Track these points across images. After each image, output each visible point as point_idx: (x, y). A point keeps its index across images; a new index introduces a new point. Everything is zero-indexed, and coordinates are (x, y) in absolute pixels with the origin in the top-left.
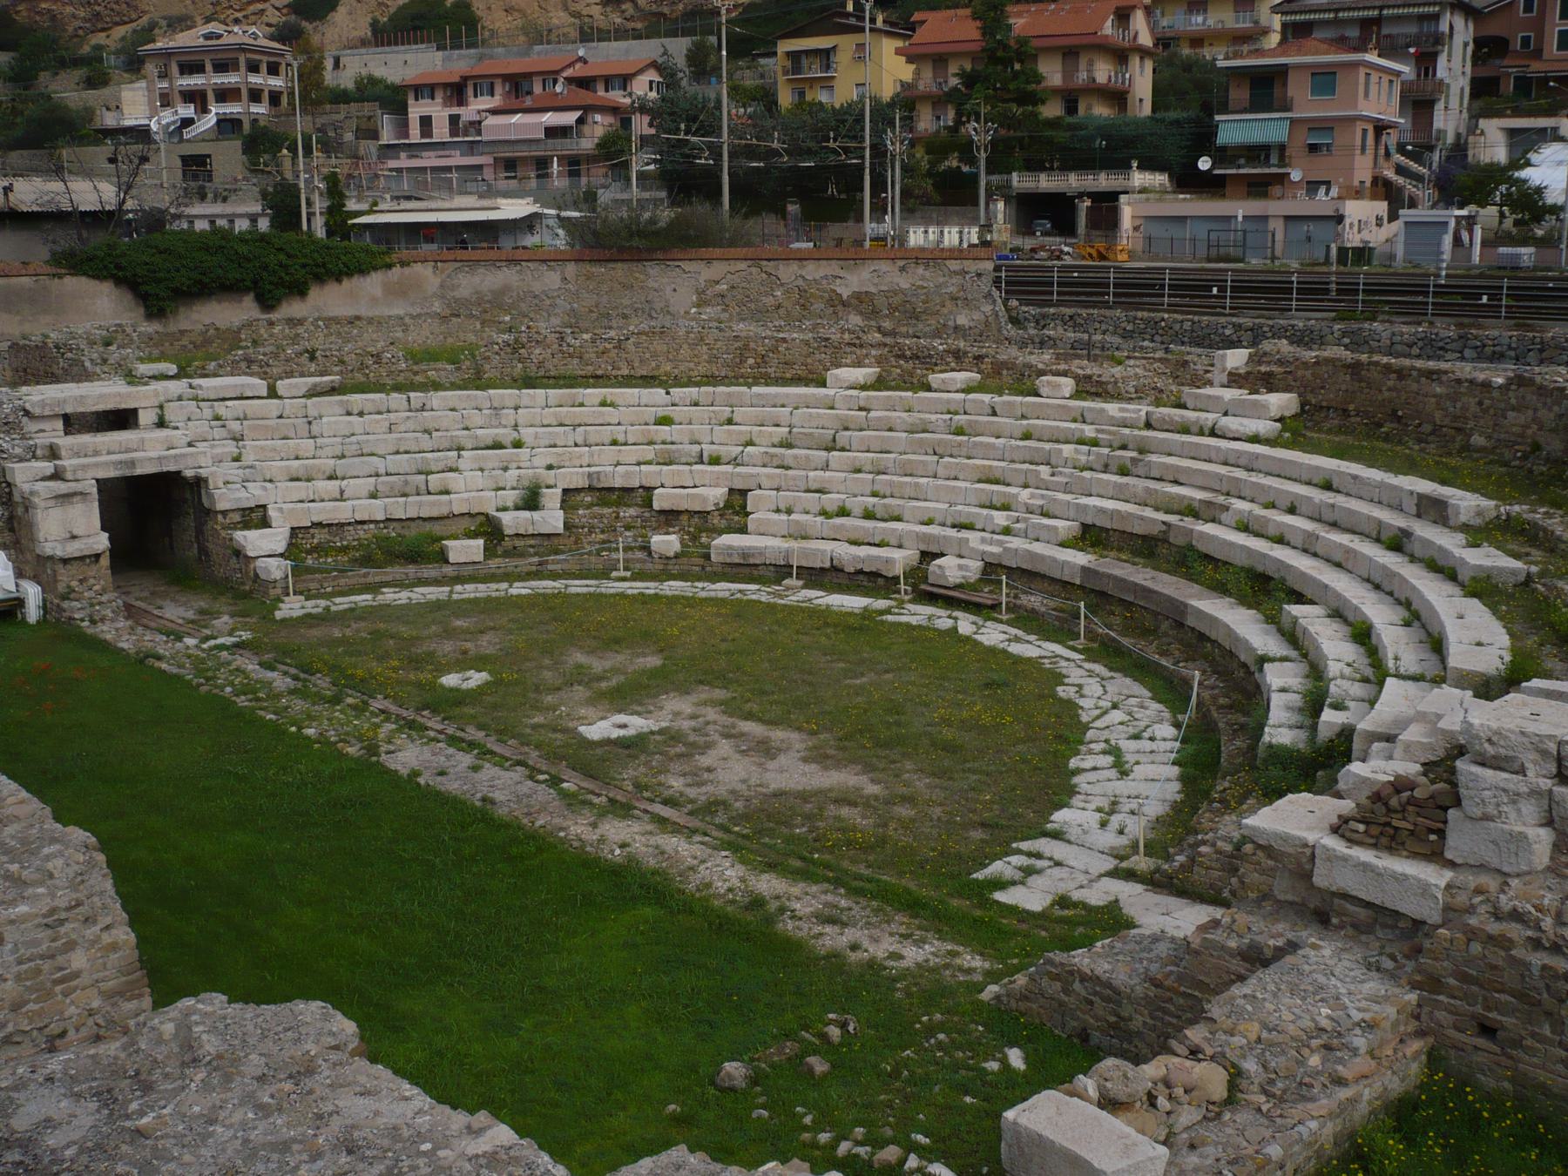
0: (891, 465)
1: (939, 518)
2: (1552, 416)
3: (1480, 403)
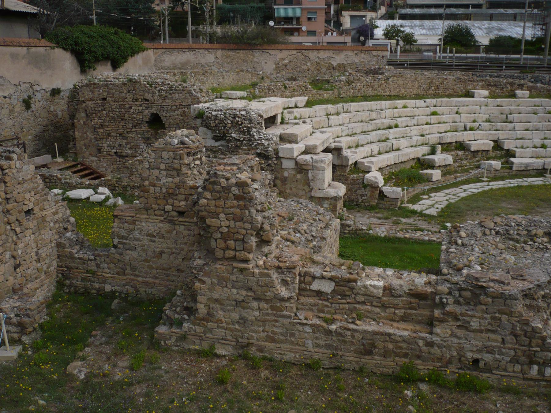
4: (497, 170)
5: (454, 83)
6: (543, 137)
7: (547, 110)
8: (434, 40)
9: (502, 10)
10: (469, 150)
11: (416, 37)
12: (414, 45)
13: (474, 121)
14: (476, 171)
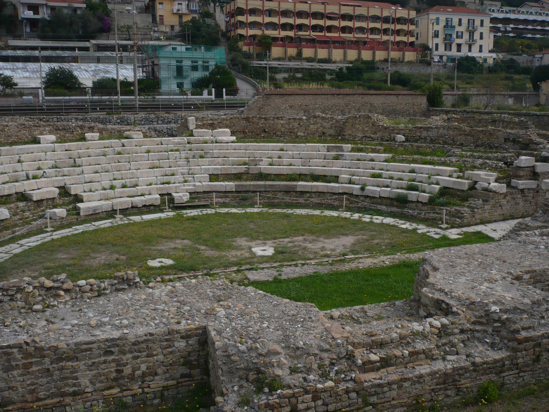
0: (110, 168)
1: (154, 182)
2: (329, 124)
3: (299, 124)
4: (63, 218)
5: (17, 130)
6: (112, 178)
7: (116, 151)
8: (36, 83)
9: (108, 53)
10: (31, 200)
11: (15, 81)
12: (14, 88)
13: (39, 169)
14: (39, 222)
